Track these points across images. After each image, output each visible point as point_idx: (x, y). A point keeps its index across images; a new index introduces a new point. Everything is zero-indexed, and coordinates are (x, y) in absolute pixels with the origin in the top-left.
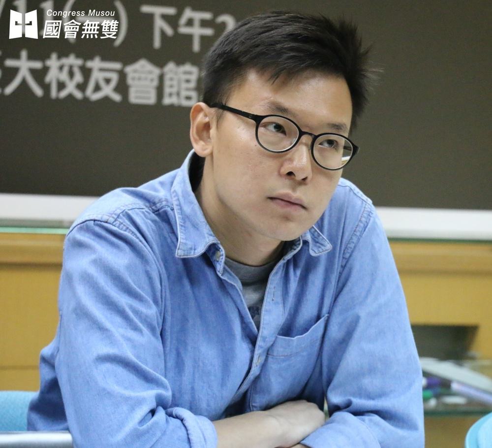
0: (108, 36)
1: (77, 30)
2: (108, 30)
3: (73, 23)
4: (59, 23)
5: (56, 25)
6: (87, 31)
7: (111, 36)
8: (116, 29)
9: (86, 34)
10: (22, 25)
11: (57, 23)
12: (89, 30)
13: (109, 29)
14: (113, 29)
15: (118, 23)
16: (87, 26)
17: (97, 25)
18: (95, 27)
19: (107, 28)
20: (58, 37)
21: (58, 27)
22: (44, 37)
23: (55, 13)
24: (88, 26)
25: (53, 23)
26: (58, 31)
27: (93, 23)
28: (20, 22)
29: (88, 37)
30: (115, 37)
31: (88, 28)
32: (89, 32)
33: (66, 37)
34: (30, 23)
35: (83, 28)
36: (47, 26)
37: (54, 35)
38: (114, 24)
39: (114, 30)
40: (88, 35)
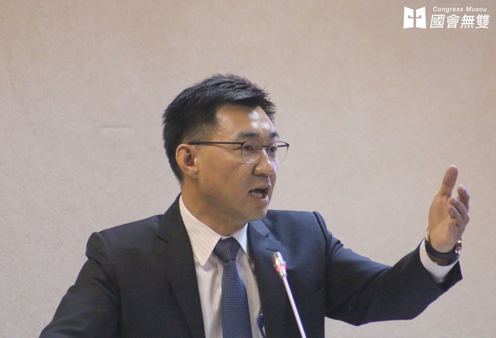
0: (481, 27)
1: (457, 22)
3: (454, 16)
4: (443, 17)
6: (465, 22)
7: (484, 27)
9: (464, 25)
10: (414, 18)
17: (472, 18)
19: (481, 20)
20: (442, 27)
21: (442, 19)
22: (431, 27)
23: (440, 10)
25: (438, 17)
26: (442, 22)
27: (470, 17)
28: (412, 15)
29: (465, 27)
30: (487, 28)
32: (466, 23)
33: (448, 27)
34: (420, 17)
35: (462, 20)
37: (438, 26)
39: (486, 22)
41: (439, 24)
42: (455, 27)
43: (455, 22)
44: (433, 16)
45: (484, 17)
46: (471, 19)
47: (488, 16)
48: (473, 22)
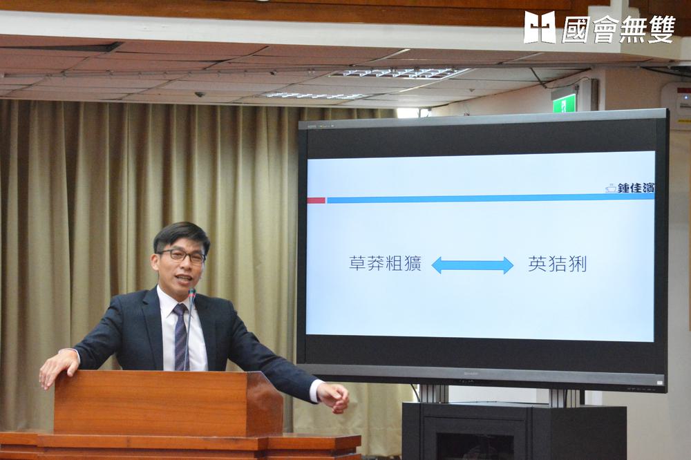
0: (659, 40)
2: (660, 31)
5: (582, 24)
6: (629, 32)
7: (664, 40)
8: (671, 29)
9: (627, 36)
11: (584, 21)
12: (631, 30)
13: (662, 29)
14: (667, 29)
15: (674, 19)
16: (628, 23)
17: (643, 23)
18: (640, 27)
19: (658, 27)
20: (585, 41)
21: (585, 26)
24: (631, 22)
25: (576, 21)
30: (670, 42)
31: (630, 27)
32: (631, 34)
33: (597, 41)
36: (568, 26)
38: (668, 21)
39: (669, 31)
40: (629, 38)
41: (579, 35)
42: (610, 41)
43: (609, 30)
44: (568, 18)
45: (665, 21)
46: (640, 24)
47: (672, 18)
48: (644, 30)
